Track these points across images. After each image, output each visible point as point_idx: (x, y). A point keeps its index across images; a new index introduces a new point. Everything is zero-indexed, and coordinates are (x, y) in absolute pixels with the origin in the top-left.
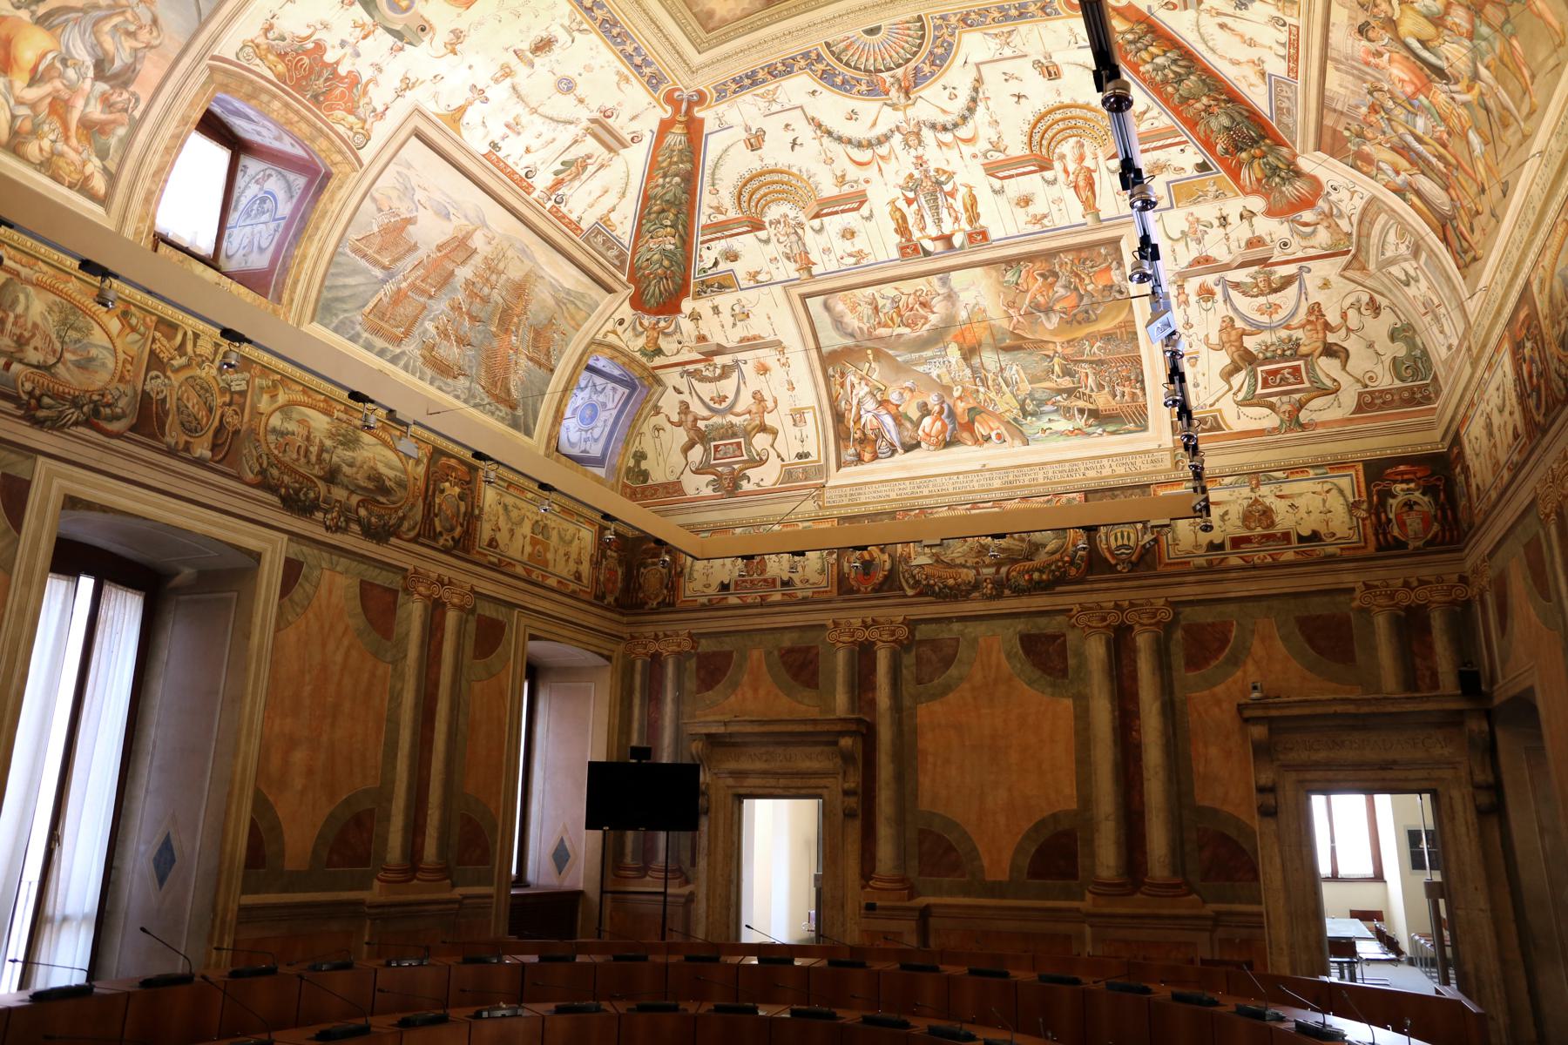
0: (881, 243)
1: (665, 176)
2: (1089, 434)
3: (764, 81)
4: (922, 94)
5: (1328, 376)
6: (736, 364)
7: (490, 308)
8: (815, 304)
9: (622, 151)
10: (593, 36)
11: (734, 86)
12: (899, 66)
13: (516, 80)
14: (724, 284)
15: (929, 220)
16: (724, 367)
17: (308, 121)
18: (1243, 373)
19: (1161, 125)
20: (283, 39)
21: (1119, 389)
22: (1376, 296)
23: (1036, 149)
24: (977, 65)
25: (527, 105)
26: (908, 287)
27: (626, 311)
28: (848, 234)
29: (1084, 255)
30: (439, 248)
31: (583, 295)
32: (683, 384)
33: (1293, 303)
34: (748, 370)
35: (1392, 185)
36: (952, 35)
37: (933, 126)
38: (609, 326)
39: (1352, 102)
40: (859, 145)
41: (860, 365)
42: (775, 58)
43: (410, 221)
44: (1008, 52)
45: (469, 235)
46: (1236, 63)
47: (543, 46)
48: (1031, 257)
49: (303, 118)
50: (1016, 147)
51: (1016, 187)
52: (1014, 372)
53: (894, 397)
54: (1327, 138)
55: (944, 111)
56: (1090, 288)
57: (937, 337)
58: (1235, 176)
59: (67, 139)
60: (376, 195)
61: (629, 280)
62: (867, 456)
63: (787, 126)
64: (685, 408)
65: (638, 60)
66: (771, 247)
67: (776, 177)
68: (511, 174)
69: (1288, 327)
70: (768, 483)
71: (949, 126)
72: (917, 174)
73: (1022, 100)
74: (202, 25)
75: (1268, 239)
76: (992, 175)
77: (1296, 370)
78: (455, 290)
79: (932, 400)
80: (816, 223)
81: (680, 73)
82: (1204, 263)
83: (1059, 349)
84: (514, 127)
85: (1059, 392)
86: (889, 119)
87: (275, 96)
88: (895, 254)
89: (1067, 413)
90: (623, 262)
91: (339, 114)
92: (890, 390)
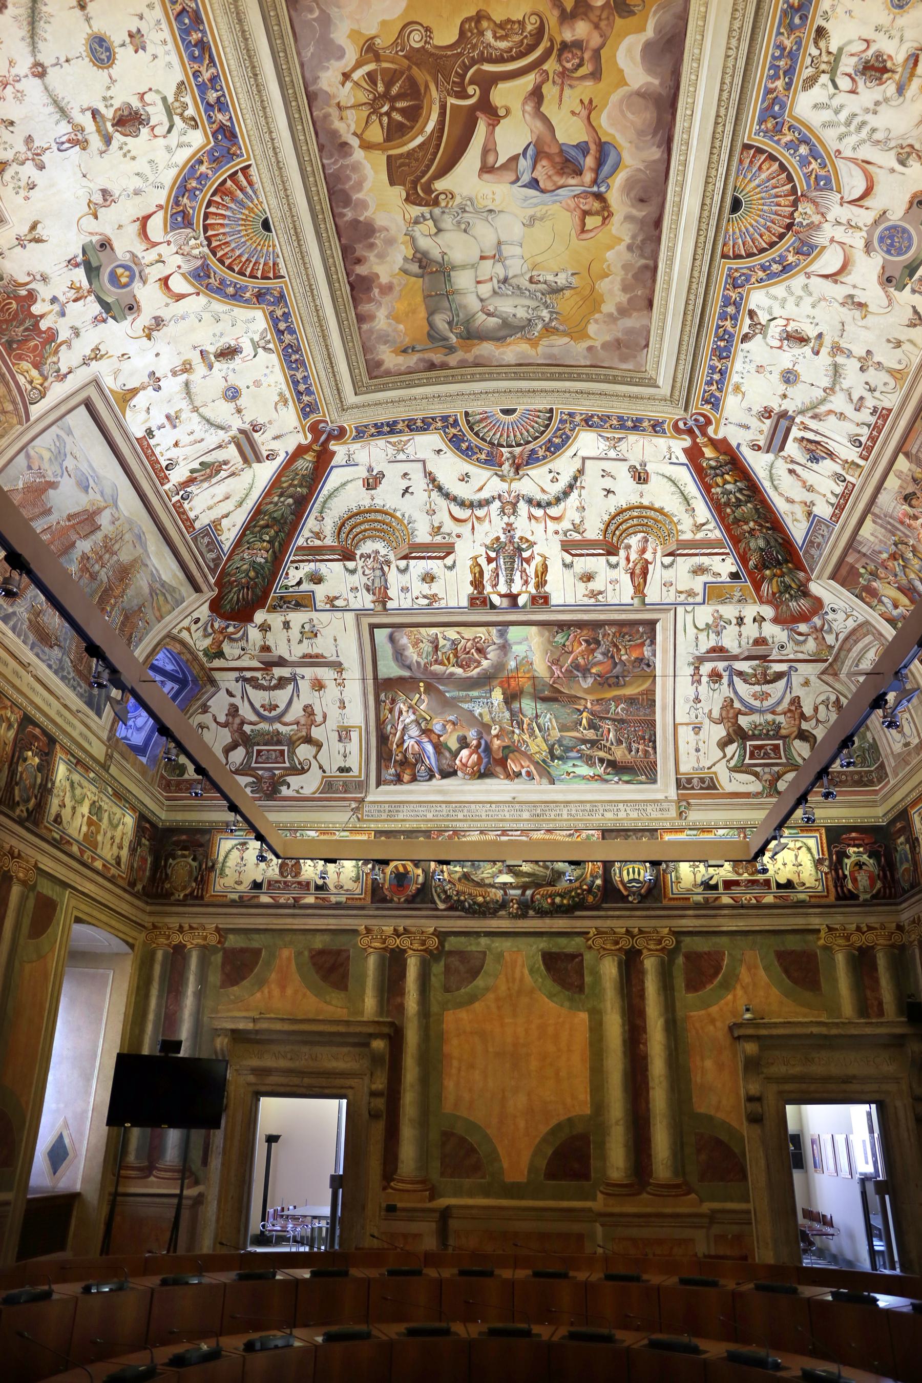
0: (455, 589)
1: (281, 496)
2: (607, 781)
3: (401, 432)
4: (529, 472)
5: (800, 755)
6: (293, 679)
7: (94, 585)
8: (381, 635)
9: (255, 465)
10: (274, 358)
11: (373, 430)
12: (519, 445)
13: (192, 377)
14: (303, 602)
15: (502, 579)
16: (281, 679)
18: (735, 745)
19: (713, 537)
21: (634, 746)
22: (842, 698)
23: (609, 536)
24: (584, 459)
26: (468, 633)
27: (204, 612)
28: (429, 578)
29: (625, 630)
30: (70, 517)
31: (174, 589)
32: (237, 688)
33: (780, 694)
34: (304, 685)
35: (887, 615)
36: (572, 430)
37: (530, 501)
38: (186, 623)
39: (877, 548)
40: (462, 504)
41: (411, 696)
42: (418, 415)
43: (53, 485)
44: (612, 454)
45: (98, 512)
46: (790, 501)
47: (228, 353)
48: (580, 625)
50: (593, 532)
51: (583, 564)
52: (547, 719)
53: (437, 728)
54: (844, 571)
55: (543, 491)
56: (624, 658)
57: (485, 681)
58: (757, 587)
60: (32, 453)
61: (216, 584)
62: (406, 778)
63: (406, 474)
64: (234, 711)
65: (302, 387)
66: (356, 576)
67: (379, 517)
68: (154, 463)
69: (773, 713)
70: (307, 792)
71: (543, 504)
72: (503, 539)
73: (610, 495)
75: (770, 641)
76: (567, 551)
77: (776, 748)
78: (71, 561)
79: (472, 735)
80: (402, 564)
81: (332, 408)
82: (719, 652)
83: (589, 705)
84: (172, 420)
85: (584, 742)
86: (495, 486)
88: (464, 603)
89: (589, 761)
90: (217, 566)
91: (25, 365)
92: (435, 721)
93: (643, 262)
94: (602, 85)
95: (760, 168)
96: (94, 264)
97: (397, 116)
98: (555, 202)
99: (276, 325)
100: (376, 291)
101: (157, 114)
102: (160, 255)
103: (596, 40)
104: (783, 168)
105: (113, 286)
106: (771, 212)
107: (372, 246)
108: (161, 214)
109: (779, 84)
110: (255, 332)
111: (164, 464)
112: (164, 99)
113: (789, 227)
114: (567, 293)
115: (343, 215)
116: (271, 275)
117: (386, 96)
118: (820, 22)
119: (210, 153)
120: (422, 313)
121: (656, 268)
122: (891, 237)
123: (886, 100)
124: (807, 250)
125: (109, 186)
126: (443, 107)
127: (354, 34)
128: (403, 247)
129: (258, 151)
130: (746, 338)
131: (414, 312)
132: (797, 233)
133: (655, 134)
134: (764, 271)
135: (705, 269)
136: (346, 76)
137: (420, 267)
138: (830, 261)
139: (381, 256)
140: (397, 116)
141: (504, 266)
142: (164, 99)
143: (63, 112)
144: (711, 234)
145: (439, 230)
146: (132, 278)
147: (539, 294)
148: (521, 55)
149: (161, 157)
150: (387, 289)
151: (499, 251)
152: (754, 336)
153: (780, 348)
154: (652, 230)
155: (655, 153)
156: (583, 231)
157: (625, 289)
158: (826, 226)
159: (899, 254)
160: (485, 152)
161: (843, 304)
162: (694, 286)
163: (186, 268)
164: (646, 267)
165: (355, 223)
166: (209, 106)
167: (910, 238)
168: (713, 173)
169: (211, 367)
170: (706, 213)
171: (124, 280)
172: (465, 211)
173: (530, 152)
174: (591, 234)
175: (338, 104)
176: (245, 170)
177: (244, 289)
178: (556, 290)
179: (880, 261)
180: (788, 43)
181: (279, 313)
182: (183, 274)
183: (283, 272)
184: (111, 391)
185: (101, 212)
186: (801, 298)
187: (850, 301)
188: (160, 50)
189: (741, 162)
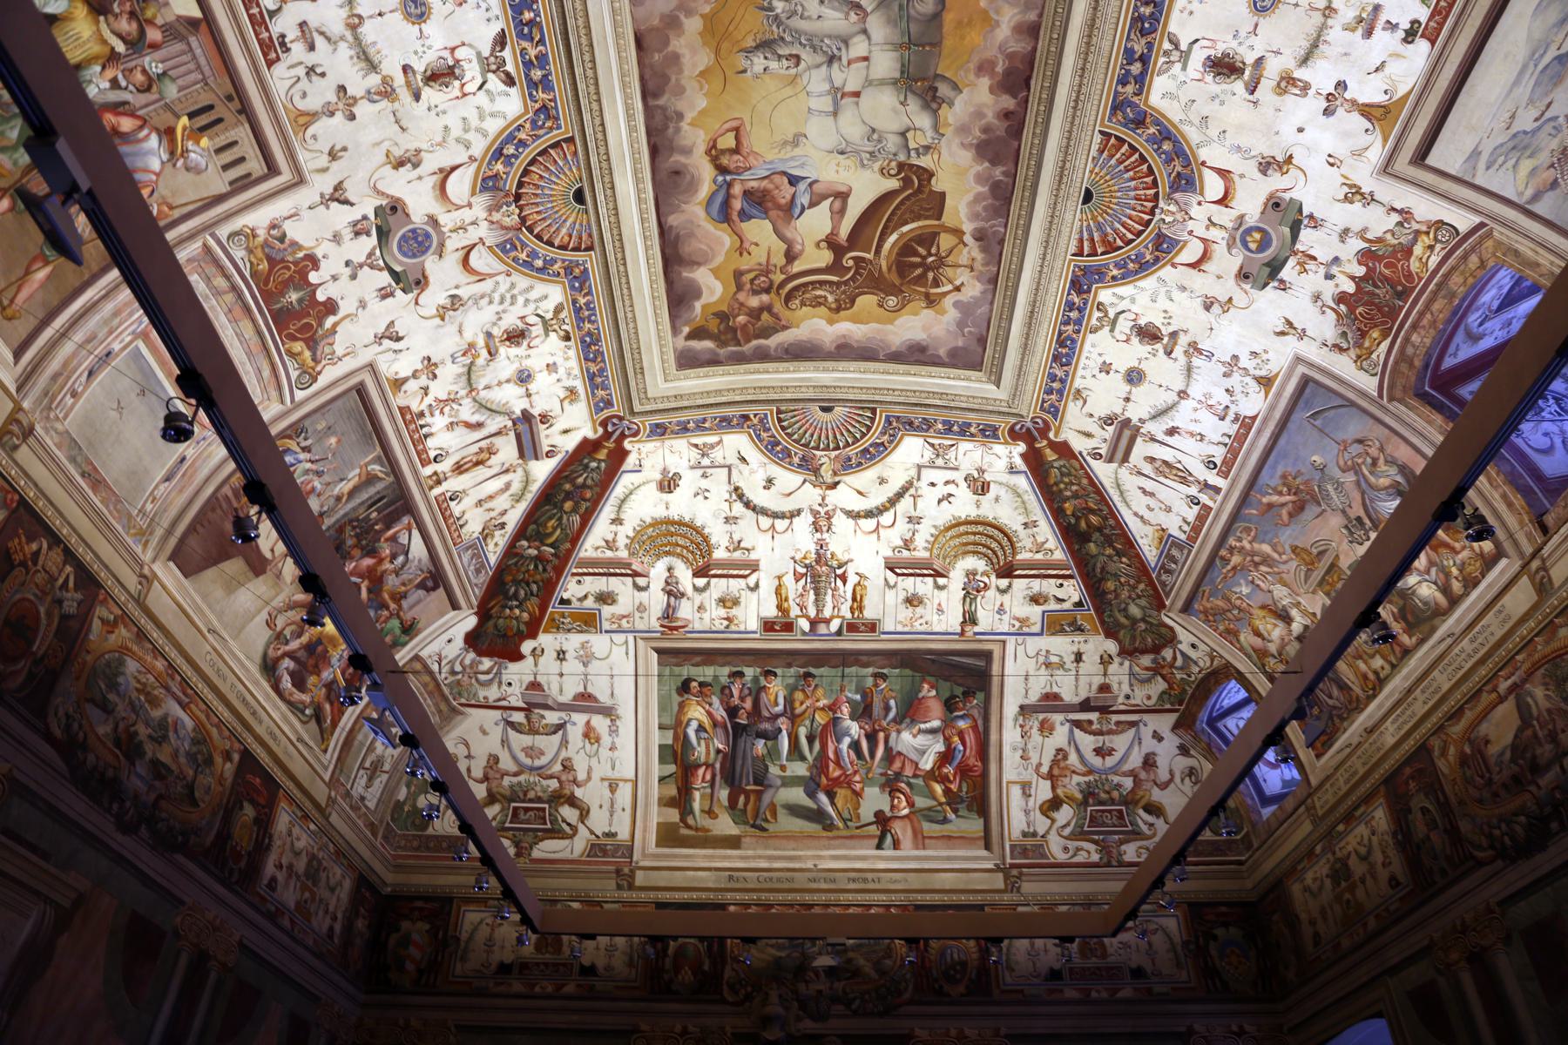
10: (1173, 27)
17: (1431, 301)
20: (1344, 334)
25: (1322, 28)
47: (1224, 67)
49: (1427, 306)
59: (1453, 550)
74: (1353, 404)
87: (1407, 340)
91: (1414, 265)
93: (661, 102)
94: (733, 267)
95: (570, 236)
96: (1268, 270)
97: (922, 251)
98: (771, 162)
99: (1143, 73)
100: (999, 69)
101: (1124, 325)
102: (1207, 228)
103: (741, 296)
104: (550, 243)
105: (1271, 240)
106: (542, 203)
107: (985, 130)
108: (1177, 260)
109: (582, 301)
110: (1174, 77)
111: (1196, 508)
112: (1112, 331)
113: (518, 197)
114: (750, 43)
115: (1005, 174)
116: (1113, 140)
117: (928, 268)
118: (571, 343)
119: (1100, 280)
120: (949, 18)
121: (645, 95)
122: (420, 244)
123: (495, 324)
124: (488, 183)
125: (1201, 309)
126: (878, 252)
127: (943, 312)
128: (950, 120)
129: (1058, 264)
130: (501, 41)
131: (959, 24)
132: (507, 195)
133: (678, 237)
134: (520, 141)
135: (586, 117)
136: (958, 289)
137: (936, 89)
138: (459, 186)
139: (979, 114)
140: (922, 251)
141: (831, 81)
142: (1112, 331)
143: (1189, 370)
144: (594, 159)
145: (903, 134)
146: (1249, 231)
147: (788, 39)
148: (805, 285)
149: (1143, 300)
150: (984, 68)
151: (836, 103)
152: (493, 50)
153: (453, 50)
154: (660, 140)
155: (673, 220)
156: (737, 130)
157: (675, 58)
158: (485, 215)
159: (404, 236)
160: (842, 211)
161: (418, 151)
162: (592, 89)
163: (1194, 199)
164: (656, 96)
165: (994, 162)
166: (1080, 310)
167: (405, 255)
168: (613, 219)
169: (1259, 61)
170: (607, 180)
171: (1257, 236)
172: (871, 154)
173: (797, 211)
174: (727, 126)
175: (972, 270)
176: (1080, 253)
177: (1152, 140)
178: (766, 46)
179: (413, 218)
180: (588, 325)
181: (1130, 89)
182: (1202, 194)
183: (1098, 138)
184: (1385, 140)
185: (1224, 299)
186: (466, 131)
187: (414, 160)
188: (1094, 356)
189: (590, 236)
